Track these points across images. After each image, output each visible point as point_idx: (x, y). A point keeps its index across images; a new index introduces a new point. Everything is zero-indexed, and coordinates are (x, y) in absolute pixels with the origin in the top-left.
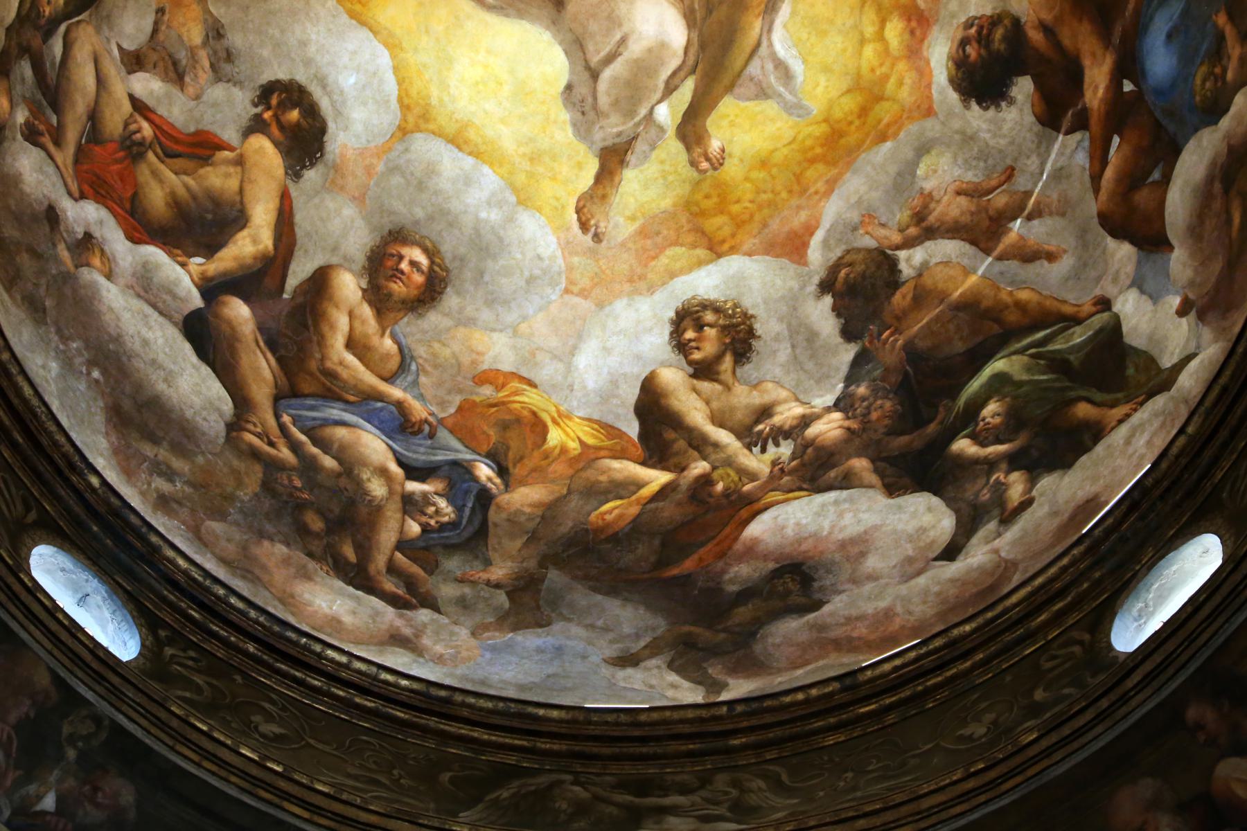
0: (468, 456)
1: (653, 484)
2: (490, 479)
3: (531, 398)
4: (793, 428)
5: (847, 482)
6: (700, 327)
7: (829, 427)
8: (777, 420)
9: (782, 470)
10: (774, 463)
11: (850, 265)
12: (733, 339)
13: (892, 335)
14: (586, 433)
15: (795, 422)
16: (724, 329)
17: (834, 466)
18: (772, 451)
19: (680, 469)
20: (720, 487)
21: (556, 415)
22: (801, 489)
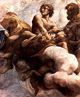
0: (4, 30)
1: (32, 37)
2: (7, 34)
3: (16, 18)
4: (56, 32)
5: (62, 46)
6: (45, 9)
7: (62, 34)
8: (54, 30)
9: (53, 39)
10: (52, 37)
11: (72, 6)
12: (50, 12)
13: (75, 22)
14: (24, 25)
15: (56, 31)
16: (49, 10)
17: (61, 42)
18: (52, 35)
19: (37, 34)
20: (43, 39)
21: (19, 21)
22: (55, 44)
